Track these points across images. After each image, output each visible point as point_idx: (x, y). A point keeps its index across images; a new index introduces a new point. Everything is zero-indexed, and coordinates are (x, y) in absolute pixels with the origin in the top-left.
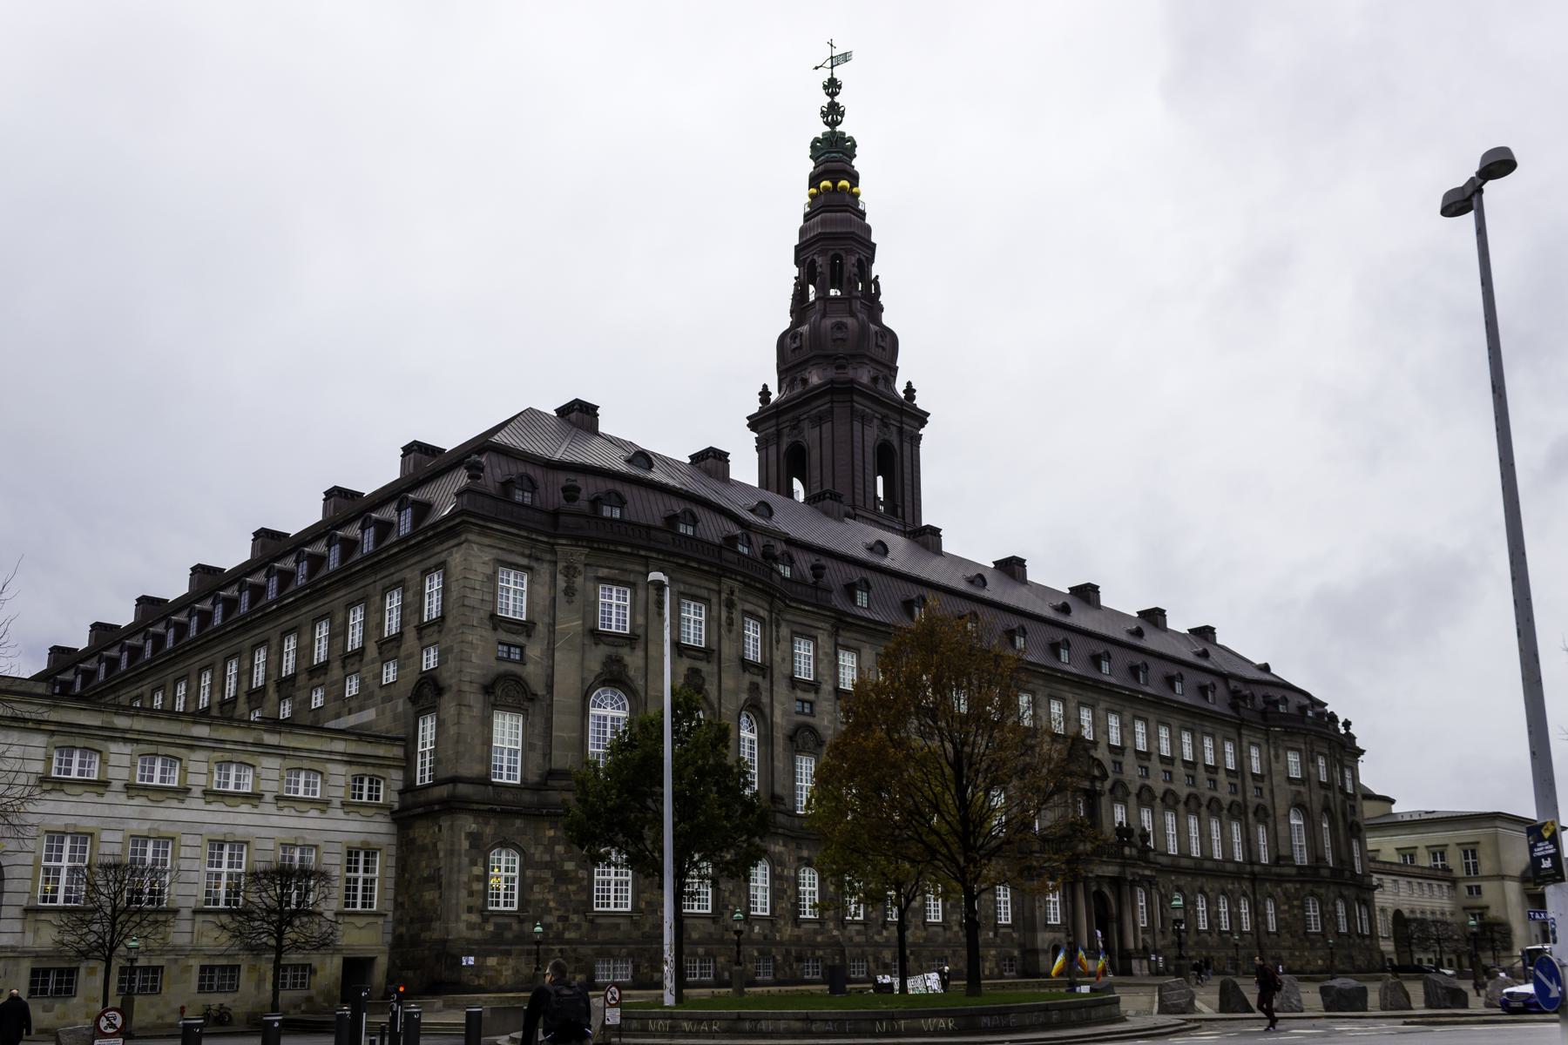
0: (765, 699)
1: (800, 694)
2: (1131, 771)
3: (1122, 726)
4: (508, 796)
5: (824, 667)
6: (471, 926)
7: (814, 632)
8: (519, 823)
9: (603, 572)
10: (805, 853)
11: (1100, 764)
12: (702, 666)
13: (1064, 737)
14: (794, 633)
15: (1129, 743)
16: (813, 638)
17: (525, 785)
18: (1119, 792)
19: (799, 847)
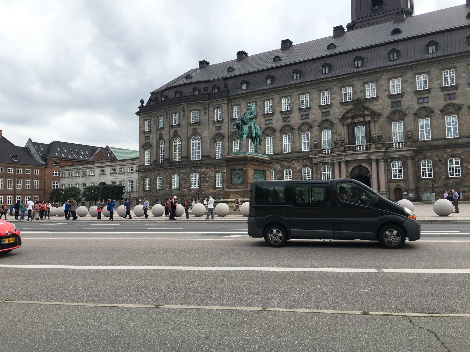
0: (199, 131)
1: (216, 125)
2: (410, 103)
3: (402, 82)
4: (147, 168)
5: (225, 115)
6: (142, 194)
7: (221, 105)
8: (149, 173)
9: (159, 115)
10: (217, 170)
11: (367, 109)
12: (178, 129)
13: (353, 101)
14: (215, 108)
15: (409, 89)
16: (221, 107)
17: (151, 165)
18: (398, 114)
19: (215, 168)
